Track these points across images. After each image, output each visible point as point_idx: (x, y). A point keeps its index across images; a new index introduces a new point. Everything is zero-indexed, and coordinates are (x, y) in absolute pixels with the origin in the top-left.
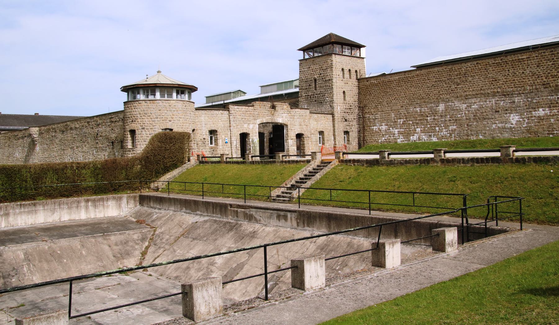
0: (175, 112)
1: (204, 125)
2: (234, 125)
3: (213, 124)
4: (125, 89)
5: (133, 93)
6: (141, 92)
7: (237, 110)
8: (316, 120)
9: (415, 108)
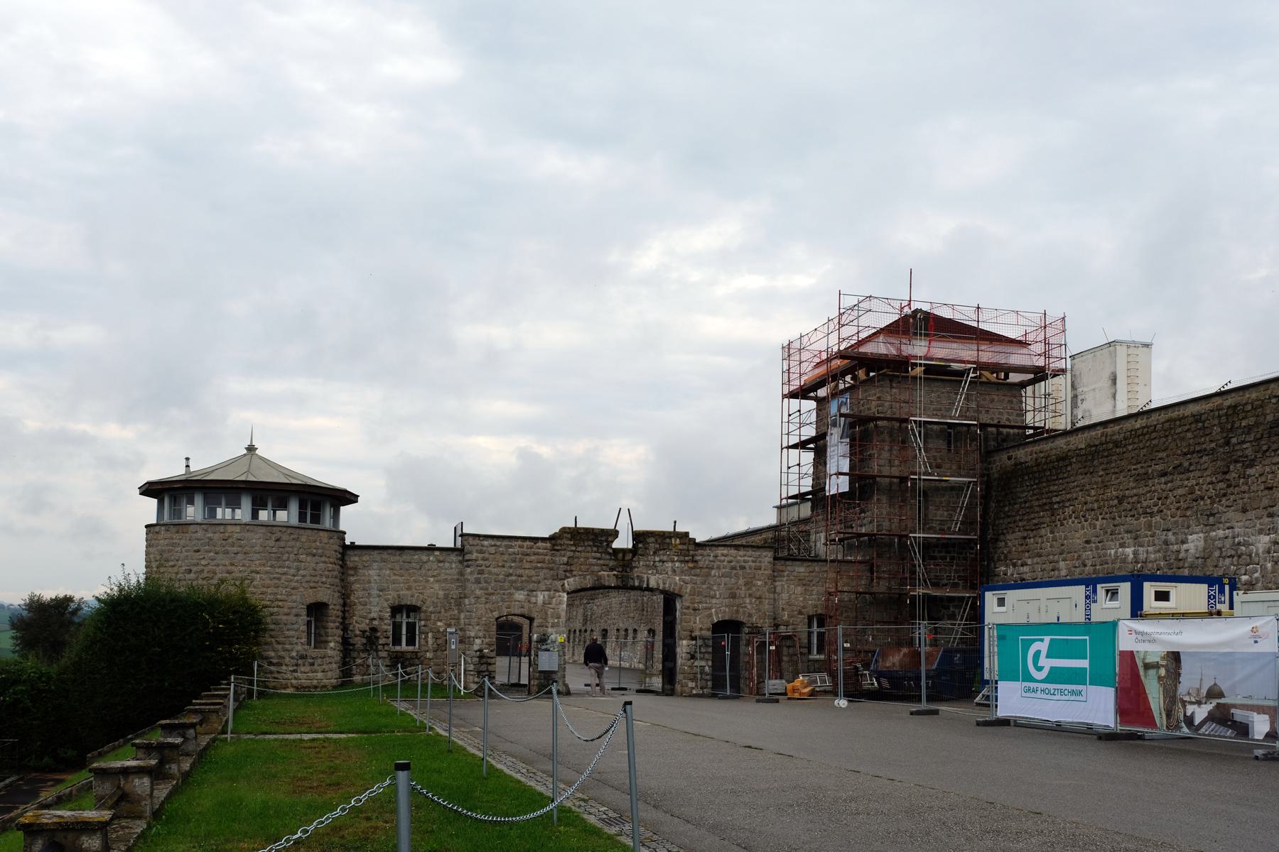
0: (240, 556)
1: (375, 592)
2: (478, 592)
3: (409, 588)
4: (150, 490)
5: (175, 501)
6: (199, 500)
7: (492, 550)
8: (801, 581)
9: (1122, 545)
